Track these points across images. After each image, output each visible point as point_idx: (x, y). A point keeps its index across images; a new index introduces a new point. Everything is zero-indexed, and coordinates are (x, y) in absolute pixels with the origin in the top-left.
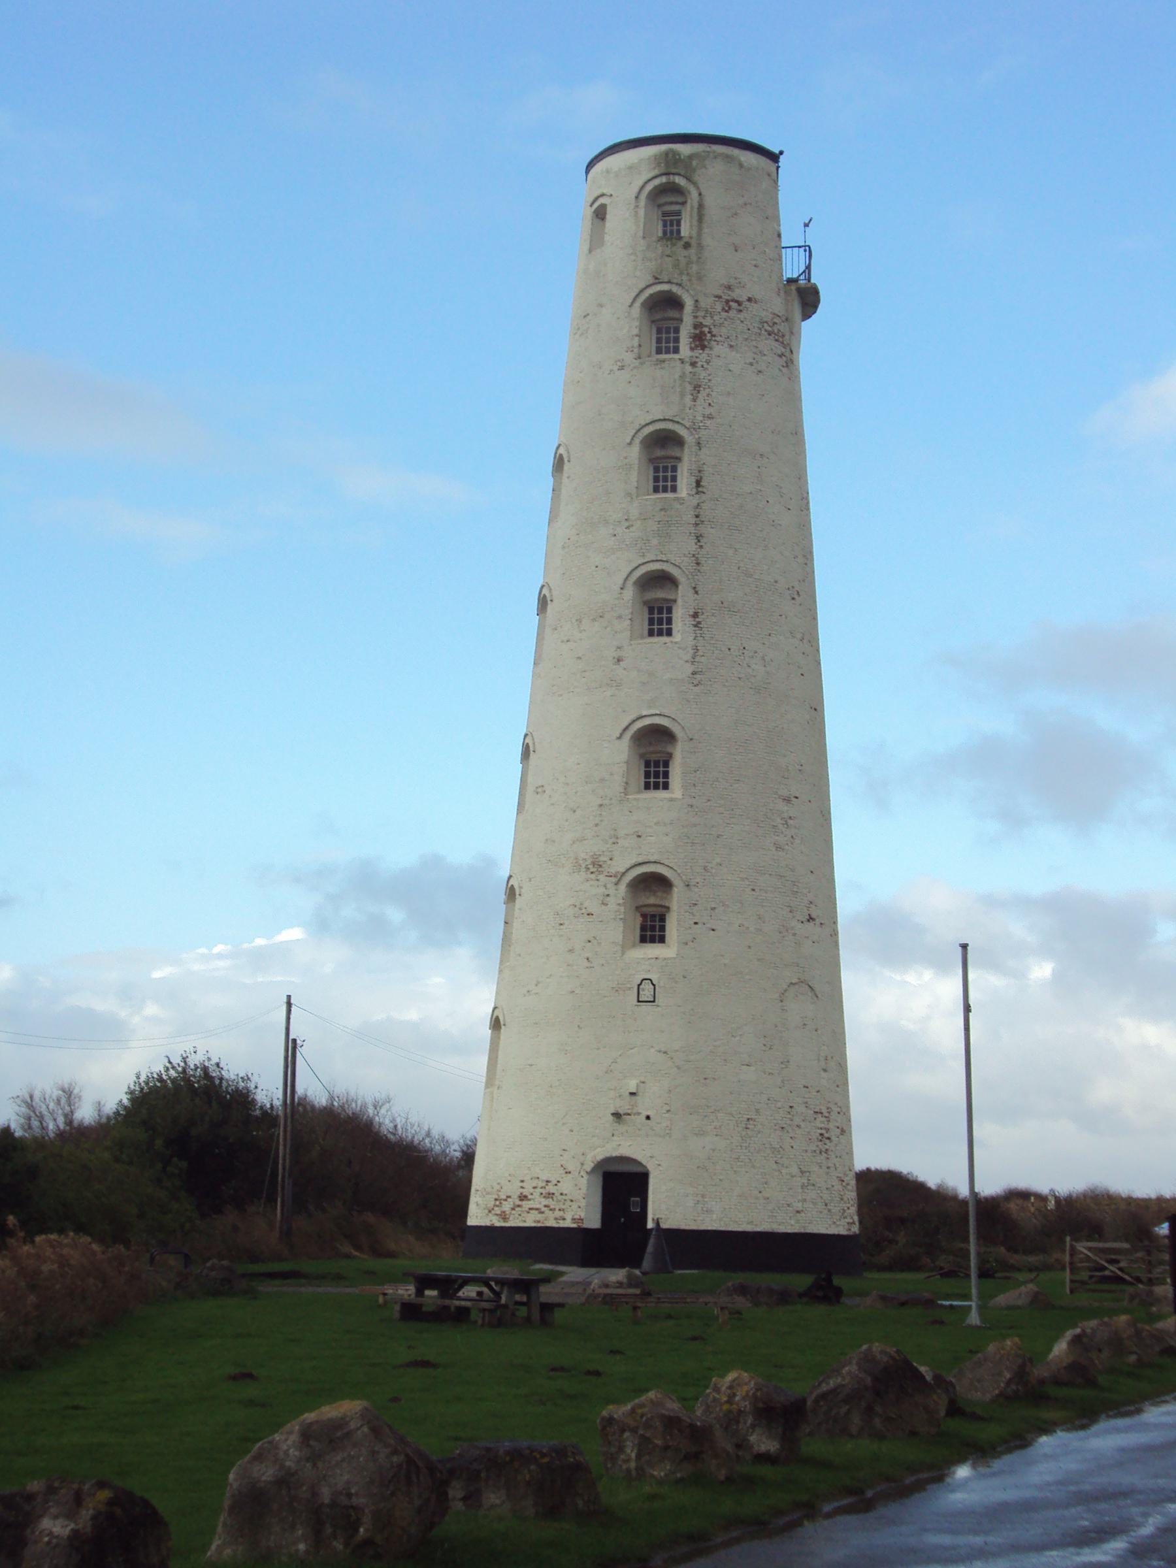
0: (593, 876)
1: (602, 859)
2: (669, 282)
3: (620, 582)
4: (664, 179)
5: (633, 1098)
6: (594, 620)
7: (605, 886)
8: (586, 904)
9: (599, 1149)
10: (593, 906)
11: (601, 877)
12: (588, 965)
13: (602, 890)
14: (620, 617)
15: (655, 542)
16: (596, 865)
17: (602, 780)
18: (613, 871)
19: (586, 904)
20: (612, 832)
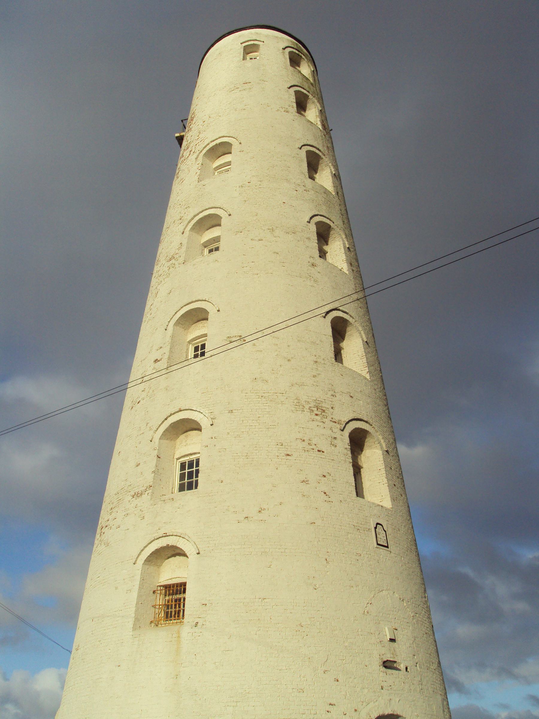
0: (318, 418)
1: (323, 405)
2: (309, 92)
3: (307, 219)
4: (297, 52)
5: (392, 644)
6: (288, 233)
8: (314, 442)
9: (371, 705)
10: (324, 445)
11: (327, 421)
12: (327, 498)
13: (328, 432)
14: (309, 239)
15: (324, 208)
16: (319, 410)
17: (313, 343)
18: (336, 418)
20: (330, 386)
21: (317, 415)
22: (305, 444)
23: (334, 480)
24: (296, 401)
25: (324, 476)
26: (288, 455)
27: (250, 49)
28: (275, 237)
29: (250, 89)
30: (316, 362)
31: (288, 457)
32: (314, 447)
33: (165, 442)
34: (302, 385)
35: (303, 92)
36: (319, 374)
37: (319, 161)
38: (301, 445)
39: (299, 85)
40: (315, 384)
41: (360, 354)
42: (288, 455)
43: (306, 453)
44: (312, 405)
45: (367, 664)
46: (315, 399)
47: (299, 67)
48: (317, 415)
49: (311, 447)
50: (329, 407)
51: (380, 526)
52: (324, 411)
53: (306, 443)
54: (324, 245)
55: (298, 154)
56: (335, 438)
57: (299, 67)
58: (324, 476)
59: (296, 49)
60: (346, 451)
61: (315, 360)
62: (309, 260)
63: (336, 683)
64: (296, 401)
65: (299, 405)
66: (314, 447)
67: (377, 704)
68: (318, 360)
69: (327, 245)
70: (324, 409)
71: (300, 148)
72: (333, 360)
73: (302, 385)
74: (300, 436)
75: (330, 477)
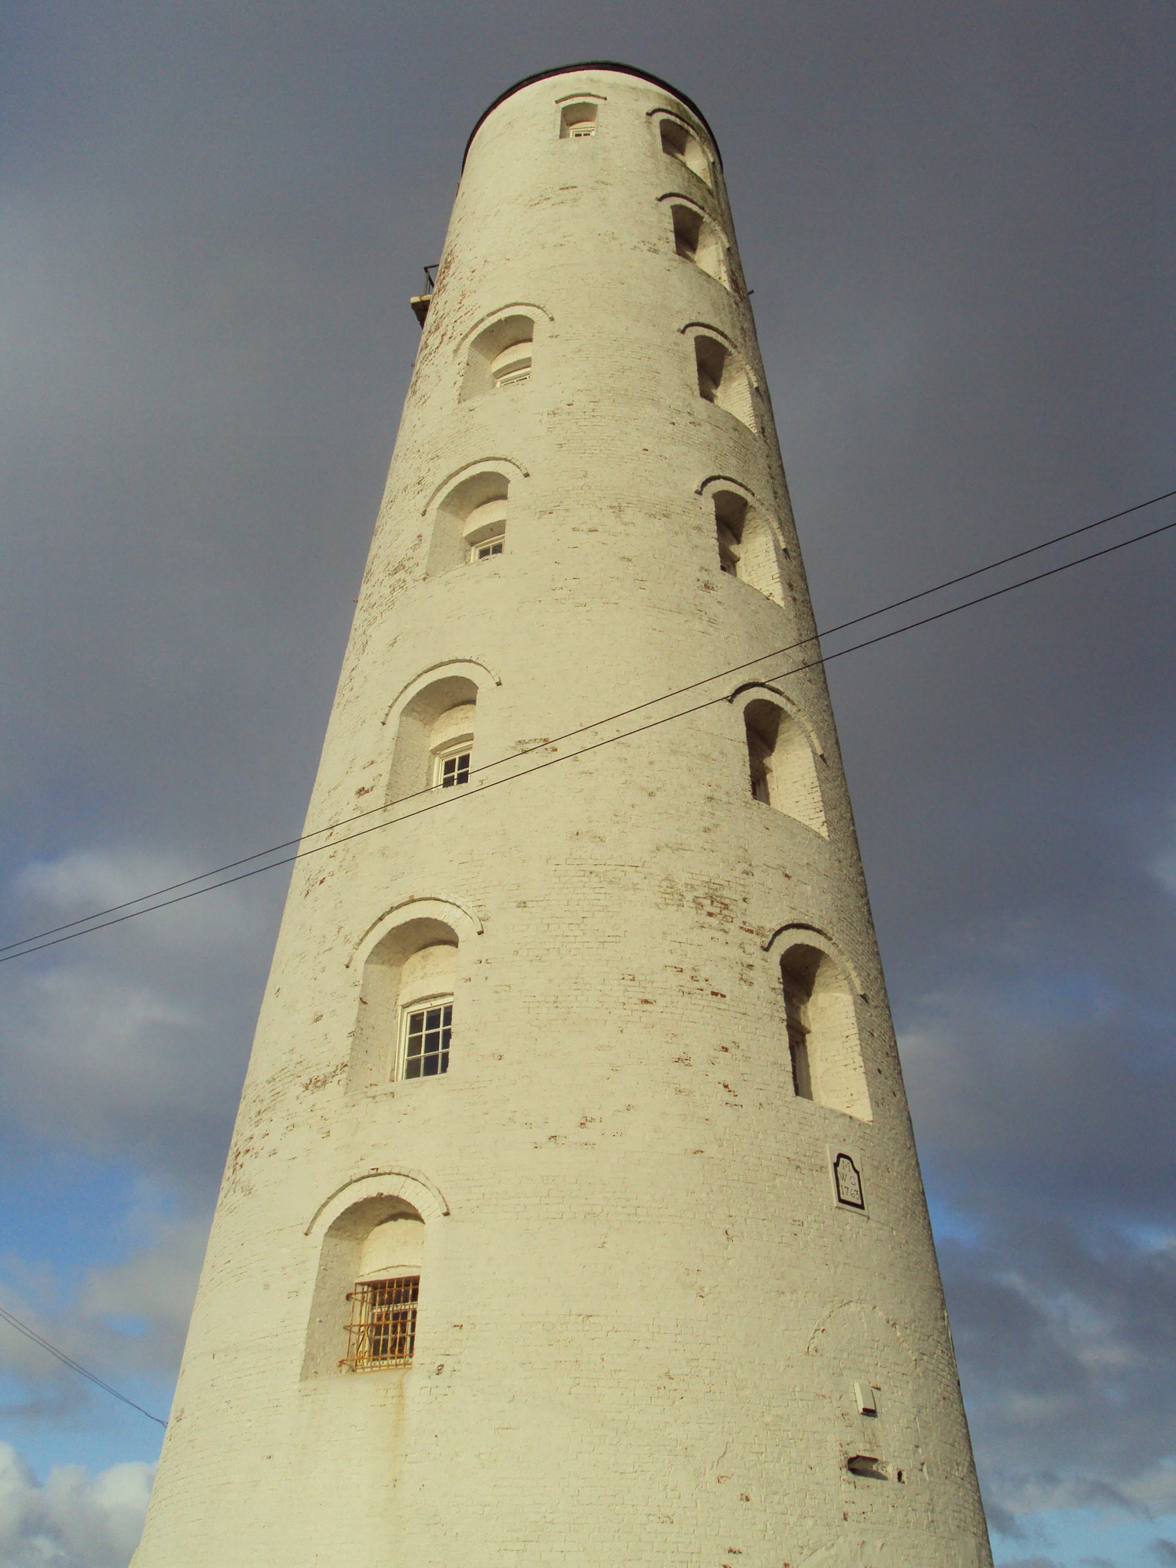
0: (713, 921)
1: (725, 893)
2: (702, 208)
3: (696, 486)
4: (678, 121)
7: (741, 946)
8: (703, 973)
9: (821, 1554)
10: (725, 981)
11: (733, 928)
12: (729, 1097)
13: (734, 953)
14: (698, 528)
15: (733, 461)
16: (716, 904)
17: (706, 757)
18: (754, 923)
19: (703, 973)
20: (740, 852)
21: (710, 914)
22: (685, 978)
23: (747, 1059)
24: (665, 884)
25: (726, 1050)
26: (646, 1002)
27: (575, 115)
28: (625, 524)
29: (575, 200)
30: (711, 799)
31: (646, 1007)
32: (702, 984)
33: (377, 968)
34: (679, 848)
35: (690, 210)
36: (716, 826)
37: (723, 359)
38: (674, 980)
39: (682, 192)
40: (707, 846)
41: (808, 782)
42: (646, 1002)
43: (687, 998)
44: (700, 892)
45: (813, 1464)
46: (706, 879)
47: (683, 153)
48: (710, 914)
49: (698, 985)
50: (738, 897)
51: (847, 1161)
52: (726, 907)
53: (685, 978)
54: (732, 543)
55: (677, 344)
56: (750, 966)
57: (683, 153)
58: (726, 1050)
59: (677, 116)
60: (774, 995)
61: (709, 794)
62: (698, 575)
63: (745, 1503)
64: (665, 884)
65: (672, 893)
66: (702, 984)
67: (833, 1551)
68: (716, 795)
69: (739, 542)
70: (727, 901)
71: (683, 332)
72: (749, 794)
73: (679, 848)
74: (671, 960)
75: (739, 1053)
